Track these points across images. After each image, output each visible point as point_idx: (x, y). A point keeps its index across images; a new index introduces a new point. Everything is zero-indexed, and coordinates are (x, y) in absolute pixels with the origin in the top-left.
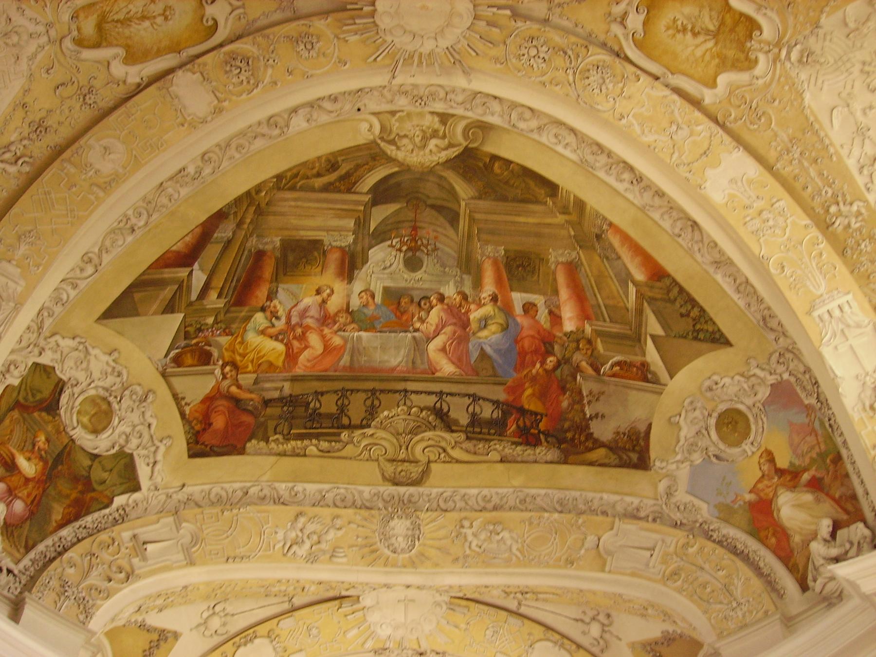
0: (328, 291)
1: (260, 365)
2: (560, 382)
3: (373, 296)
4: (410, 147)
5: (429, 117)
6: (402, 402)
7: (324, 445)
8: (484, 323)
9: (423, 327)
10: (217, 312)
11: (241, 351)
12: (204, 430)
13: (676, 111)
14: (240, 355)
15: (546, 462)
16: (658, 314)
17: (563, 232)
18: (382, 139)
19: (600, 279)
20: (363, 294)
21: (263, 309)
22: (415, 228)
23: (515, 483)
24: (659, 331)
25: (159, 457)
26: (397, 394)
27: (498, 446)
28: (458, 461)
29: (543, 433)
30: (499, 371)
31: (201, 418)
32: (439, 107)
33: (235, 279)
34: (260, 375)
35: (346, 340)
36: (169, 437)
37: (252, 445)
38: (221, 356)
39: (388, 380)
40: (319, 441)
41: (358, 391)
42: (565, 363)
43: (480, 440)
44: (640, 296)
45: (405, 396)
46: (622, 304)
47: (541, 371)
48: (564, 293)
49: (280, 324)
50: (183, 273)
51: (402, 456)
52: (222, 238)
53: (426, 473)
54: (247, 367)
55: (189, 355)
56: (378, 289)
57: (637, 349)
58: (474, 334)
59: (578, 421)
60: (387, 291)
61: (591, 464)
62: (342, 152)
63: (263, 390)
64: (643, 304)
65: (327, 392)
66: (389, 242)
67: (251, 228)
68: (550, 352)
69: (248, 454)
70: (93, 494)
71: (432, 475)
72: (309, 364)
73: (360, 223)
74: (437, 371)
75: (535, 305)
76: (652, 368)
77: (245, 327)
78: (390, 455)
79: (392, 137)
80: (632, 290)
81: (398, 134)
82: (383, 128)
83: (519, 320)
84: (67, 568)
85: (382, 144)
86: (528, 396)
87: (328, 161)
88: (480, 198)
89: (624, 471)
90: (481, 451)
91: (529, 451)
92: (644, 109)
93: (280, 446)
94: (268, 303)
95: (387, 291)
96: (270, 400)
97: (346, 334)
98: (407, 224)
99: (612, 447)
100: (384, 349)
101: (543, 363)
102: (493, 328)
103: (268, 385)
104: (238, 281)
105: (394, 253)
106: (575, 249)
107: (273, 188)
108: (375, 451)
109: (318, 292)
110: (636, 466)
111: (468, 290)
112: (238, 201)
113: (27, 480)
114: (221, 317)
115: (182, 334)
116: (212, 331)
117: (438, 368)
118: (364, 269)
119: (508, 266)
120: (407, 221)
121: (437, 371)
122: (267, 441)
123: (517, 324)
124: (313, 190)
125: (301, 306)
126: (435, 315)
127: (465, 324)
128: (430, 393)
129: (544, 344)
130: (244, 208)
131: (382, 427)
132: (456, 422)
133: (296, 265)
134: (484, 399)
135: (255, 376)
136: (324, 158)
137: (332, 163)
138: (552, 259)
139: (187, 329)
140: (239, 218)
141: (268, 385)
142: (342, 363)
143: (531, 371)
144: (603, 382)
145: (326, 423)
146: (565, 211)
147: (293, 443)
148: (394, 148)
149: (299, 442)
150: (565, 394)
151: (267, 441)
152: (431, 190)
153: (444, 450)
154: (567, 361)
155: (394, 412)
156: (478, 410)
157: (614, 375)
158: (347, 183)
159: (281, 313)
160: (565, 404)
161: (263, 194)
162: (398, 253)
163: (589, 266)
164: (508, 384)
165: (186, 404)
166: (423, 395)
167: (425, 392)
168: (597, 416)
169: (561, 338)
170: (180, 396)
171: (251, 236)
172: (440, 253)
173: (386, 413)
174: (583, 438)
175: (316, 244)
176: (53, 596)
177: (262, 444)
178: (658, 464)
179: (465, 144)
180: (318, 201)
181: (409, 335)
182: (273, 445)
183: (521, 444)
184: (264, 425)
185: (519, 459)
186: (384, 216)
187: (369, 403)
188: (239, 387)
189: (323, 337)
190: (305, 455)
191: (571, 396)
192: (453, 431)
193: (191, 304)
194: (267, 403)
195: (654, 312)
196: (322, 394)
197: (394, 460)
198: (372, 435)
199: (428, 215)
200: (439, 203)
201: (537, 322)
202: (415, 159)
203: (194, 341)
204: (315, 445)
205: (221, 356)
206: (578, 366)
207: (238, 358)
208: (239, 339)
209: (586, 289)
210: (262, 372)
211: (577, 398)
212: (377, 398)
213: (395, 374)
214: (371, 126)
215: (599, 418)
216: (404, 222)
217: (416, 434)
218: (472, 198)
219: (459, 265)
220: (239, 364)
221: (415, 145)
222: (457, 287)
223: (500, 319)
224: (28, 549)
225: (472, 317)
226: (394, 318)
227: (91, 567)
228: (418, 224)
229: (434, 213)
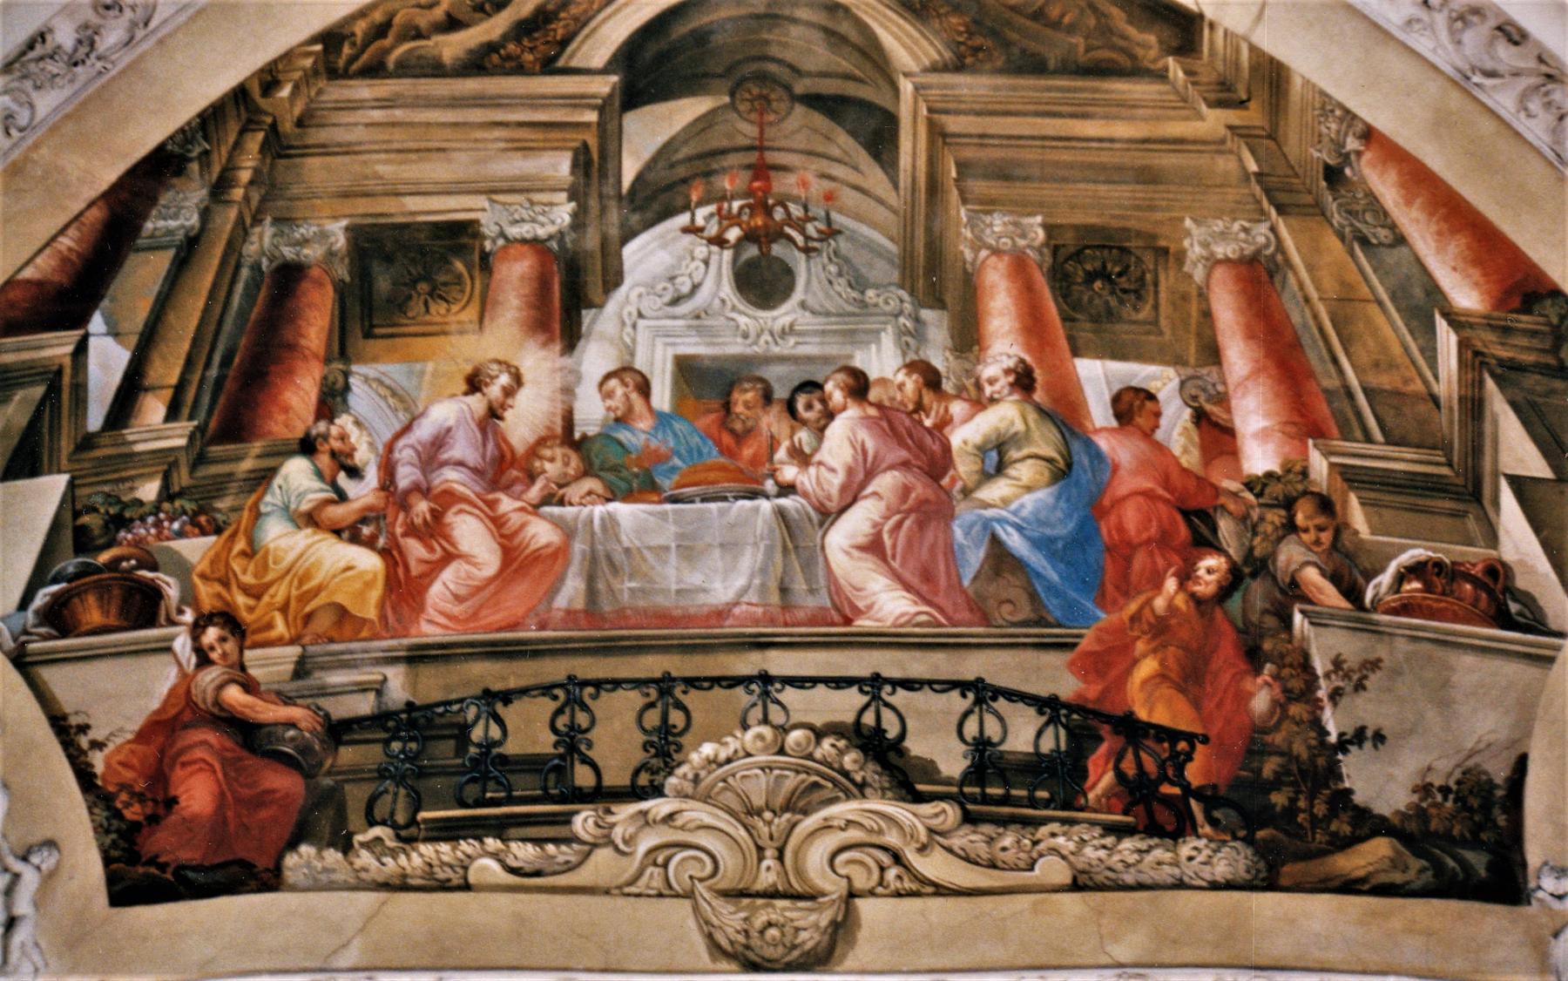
0: (504, 379)
1: (308, 618)
3: (644, 388)
6: (757, 713)
7: (524, 853)
8: (997, 456)
9: (806, 479)
10: (166, 462)
11: (248, 579)
12: (154, 820)
14: (246, 590)
15: (1215, 886)
16: (1529, 414)
17: (1225, 164)
19: (1345, 310)
20: (613, 383)
21: (307, 447)
22: (762, 171)
26: (740, 691)
27: (1061, 840)
28: (940, 890)
29: (1199, 794)
30: (1054, 607)
31: (141, 785)
33: (217, 359)
34: (312, 649)
35: (568, 531)
36: (51, 844)
37: (301, 860)
38: (189, 597)
40: (504, 840)
41: (616, 684)
42: (1254, 575)
43: (1004, 822)
45: (766, 694)
46: (1418, 386)
47: (1180, 601)
48: (1238, 356)
49: (363, 492)
50: (56, 347)
51: (768, 877)
52: (170, 232)
53: (842, 929)
54: (270, 626)
55: (91, 600)
57: (1471, 524)
58: (966, 492)
59: (1305, 755)
60: (686, 369)
61: (1349, 887)
63: (324, 691)
64: (1481, 383)
65: (524, 691)
67: (255, 197)
68: (1206, 541)
69: (293, 888)
72: (457, 610)
73: (588, 164)
74: (858, 612)
75: (1151, 397)
76: (1521, 583)
77: (256, 505)
78: (725, 881)
80: (1447, 339)
83: (1103, 443)
86: (1145, 682)
88: (959, 67)
90: (1009, 857)
93: (388, 860)
95: (686, 369)
97: (568, 511)
98: (733, 160)
99: (1410, 832)
100: (689, 551)
101: (1186, 576)
102: (1025, 471)
103: (336, 678)
104: (226, 361)
105: (701, 250)
106: (1262, 215)
107: (315, 72)
108: (682, 868)
109: (474, 383)
111: (939, 359)
112: (210, 119)
114: (183, 478)
115: (67, 537)
117: (861, 604)
118: (612, 306)
119: (1060, 278)
120: (737, 150)
121: (858, 612)
122: (346, 847)
123: (1096, 455)
124: (437, 69)
125: (424, 431)
127: (936, 464)
128: (839, 683)
129: (1186, 514)
130: (231, 139)
131: (699, 792)
132: (928, 770)
133: (398, 305)
134: (1013, 695)
135: (294, 651)
138: (1195, 251)
139: (86, 519)
140: (216, 170)
141: (336, 678)
142: (561, 601)
143: (1149, 602)
144: (1374, 630)
145: (524, 784)
146: (1225, 95)
147: (427, 849)
149: (445, 847)
150: (1258, 671)
153: (898, 859)
155: (733, 744)
156: (992, 729)
157: (1405, 609)
159: (364, 455)
160: (1261, 702)
161: (285, 92)
162: (715, 249)
163: (1311, 268)
164: (1085, 644)
165: (97, 745)
166: (821, 688)
168: (1359, 737)
169: (1235, 495)
170: (74, 721)
171: (257, 221)
172: (843, 244)
173: (708, 749)
174: (1320, 809)
175: (458, 235)
177: (333, 856)
178: (1549, 883)
180: (455, 102)
181: (765, 505)
182: (365, 858)
184: (331, 800)
185: (1129, 878)
186: (661, 140)
187: (653, 718)
188: (250, 686)
189: (497, 522)
190: (466, 887)
191: (1276, 677)
192: (920, 798)
193: (87, 442)
194: (338, 731)
196: (507, 697)
198: (671, 817)
199: (798, 127)
200: (829, 87)
201: (1161, 448)
203: (104, 557)
204: (495, 856)
205: (189, 597)
206: (1294, 583)
207: (241, 600)
208: (240, 545)
209: (1306, 341)
210: (317, 640)
211: (1296, 684)
212: (680, 706)
215: (1368, 745)
216: (723, 152)
217: (806, 812)
218: (934, 68)
219: (907, 280)
220: (245, 616)
222: (904, 354)
223: (1046, 442)
226: (713, 456)
229: (819, 120)
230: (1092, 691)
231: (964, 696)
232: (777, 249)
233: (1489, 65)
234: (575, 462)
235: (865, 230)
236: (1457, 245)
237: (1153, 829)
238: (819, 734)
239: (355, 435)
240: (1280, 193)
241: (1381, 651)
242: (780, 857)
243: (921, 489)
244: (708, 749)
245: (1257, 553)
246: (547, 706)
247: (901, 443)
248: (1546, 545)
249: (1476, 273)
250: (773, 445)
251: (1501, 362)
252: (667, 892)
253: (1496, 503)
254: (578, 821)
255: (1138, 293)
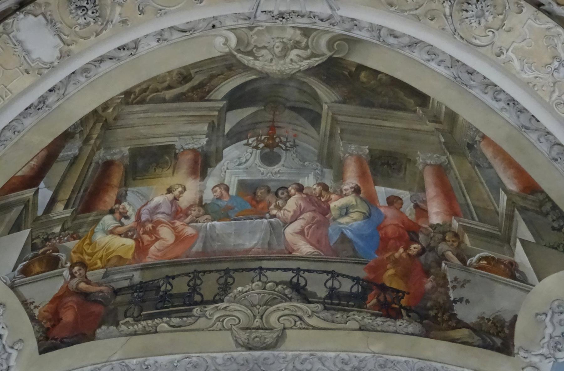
0: (180, 189)
1: (109, 260)
2: (425, 265)
3: (227, 189)
4: (270, 57)
5: (291, 31)
6: (258, 278)
7: (175, 321)
8: (346, 211)
9: (280, 214)
10: (64, 221)
11: (89, 251)
12: (54, 326)
13: (560, 45)
14: (89, 255)
15: (407, 334)
16: (529, 224)
18: (239, 51)
19: (470, 184)
20: (217, 188)
21: (112, 212)
22: (273, 128)
23: (374, 348)
24: (530, 238)
25: (12, 363)
26: (252, 272)
27: (357, 316)
28: (314, 328)
29: (405, 308)
31: (50, 316)
32: (303, 22)
33: (82, 190)
34: (109, 269)
36: (21, 340)
39: (241, 260)
40: (170, 318)
41: (211, 271)
42: (430, 251)
43: (339, 310)
44: (511, 203)
45: (260, 273)
46: (493, 208)
47: (404, 255)
48: (431, 191)
49: (129, 223)
50: (28, 193)
51: (257, 323)
52: (68, 155)
54: (96, 264)
55: (36, 265)
56: (232, 182)
58: (334, 219)
59: (442, 302)
60: (242, 184)
61: (453, 340)
62: (194, 65)
63: (113, 281)
64: (514, 211)
65: (179, 275)
66: (245, 141)
69: (99, 339)
71: (287, 340)
72: (159, 254)
73: (213, 127)
74: (294, 251)
75: (401, 199)
76: (521, 268)
77: (93, 230)
78: (242, 325)
79: (249, 49)
80: (503, 197)
81: (256, 46)
82: (240, 41)
83: (382, 210)
85: (239, 56)
86: (389, 276)
87: (180, 74)
88: (344, 102)
89: (489, 352)
90: (338, 320)
91: (389, 323)
92: (524, 44)
93: (131, 327)
94: (117, 206)
95: (242, 184)
96: (120, 289)
97: (199, 224)
99: (475, 329)
101: (406, 248)
102: (355, 216)
104: (85, 191)
105: (250, 150)
106: (444, 154)
107: (121, 102)
109: (169, 191)
110: (499, 350)
111: (329, 182)
112: (84, 121)
114: (69, 224)
115: (29, 247)
116: (60, 239)
117: (295, 249)
118: (218, 166)
120: (266, 122)
121: (294, 251)
123: (380, 213)
124: (164, 101)
125: (152, 204)
126: (292, 204)
127: (325, 211)
129: (409, 232)
130: (91, 125)
131: (235, 300)
132: (314, 295)
134: (344, 276)
135: (104, 270)
136: (176, 72)
137: (184, 76)
139: (35, 241)
140: (85, 136)
142: (194, 249)
143: (393, 255)
146: (436, 119)
147: (144, 323)
148: (251, 58)
149: (150, 322)
150: (428, 277)
151: (117, 324)
152: (292, 93)
153: (301, 319)
154: (432, 249)
155: (248, 287)
156: (336, 284)
158: (201, 92)
159: (131, 212)
160: (429, 284)
161: (110, 110)
162: (255, 150)
163: (459, 170)
164: (369, 263)
165: (36, 307)
166: (279, 271)
167: (281, 269)
168: (461, 300)
169: (426, 228)
170: (29, 301)
171: (98, 149)
172: (299, 149)
173: (240, 289)
174: (446, 317)
175: (168, 149)
177: (113, 328)
178: (522, 354)
179: (329, 54)
181: (265, 221)
182: (123, 327)
183: (381, 316)
185: (379, 329)
186: (239, 119)
187: (222, 281)
188: (88, 282)
189: (174, 229)
190: (156, 332)
191: (434, 279)
192: (310, 302)
193: (38, 219)
194: (116, 292)
195: (524, 220)
196: (173, 278)
197: (247, 329)
198: (226, 307)
199: (287, 115)
201: (402, 213)
202: (274, 67)
203: (41, 251)
204: (166, 322)
205: (69, 258)
207: (86, 257)
208: (87, 241)
210: (112, 266)
211: (442, 282)
212: (231, 277)
213: (250, 255)
214: (227, 40)
215: (464, 303)
216: (261, 123)
217: (271, 306)
218: (335, 102)
219: (320, 159)
220: (88, 262)
221: (274, 54)
222: (317, 181)
223: (363, 208)
225: (332, 205)
226: (249, 207)
228: (276, 124)
229: (295, 114)
230: (372, 276)
231: (328, 275)
232: (275, 150)
233: (528, 125)
234: (202, 211)
235: (307, 146)
236: (511, 172)
237: (388, 316)
238: (277, 284)
239: (128, 207)
240: (452, 147)
241: (470, 277)
242: (261, 318)
243: (319, 217)
244: (240, 289)
245: (432, 245)
246: (187, 279)
247: (314, 206)
248: (530, 260)
249: (516, 181)
250: (270, 204)
251: (521, 207)
252: (223, 329)
253: (515, 244)
254: (194, 311)
255: (399, 170)
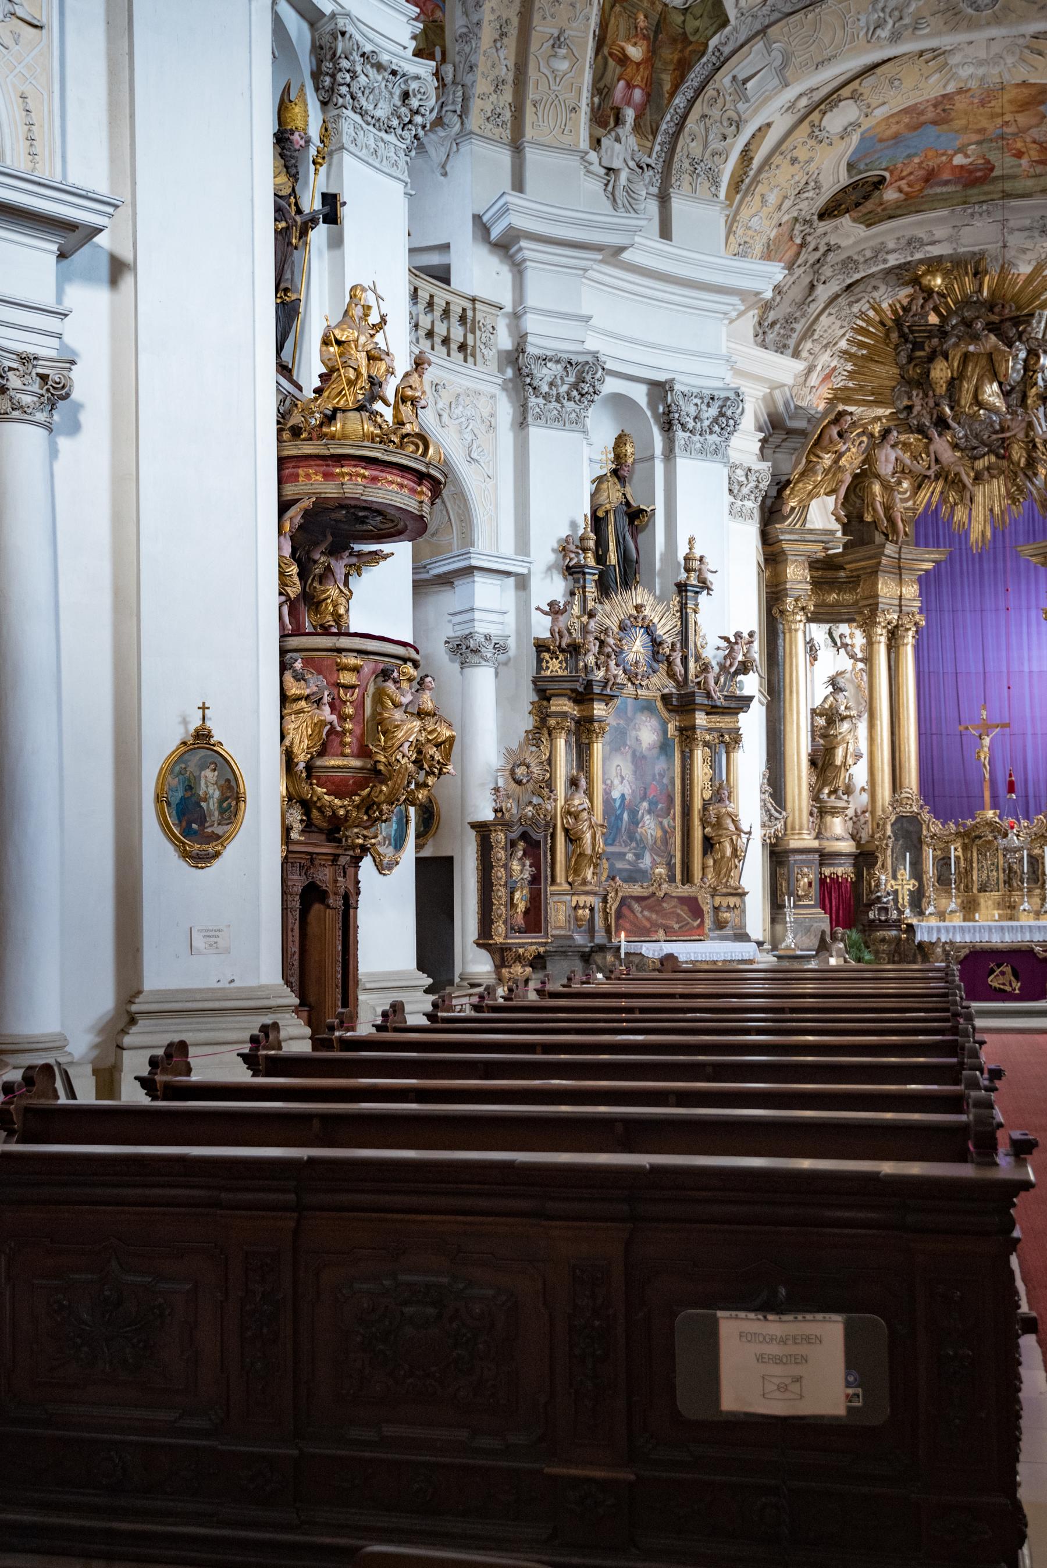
70: (690, 48)
84: (689, 146)
113: (638, 64)
176: (686, 177)
224: (654, 133)
227: (707, 130)
